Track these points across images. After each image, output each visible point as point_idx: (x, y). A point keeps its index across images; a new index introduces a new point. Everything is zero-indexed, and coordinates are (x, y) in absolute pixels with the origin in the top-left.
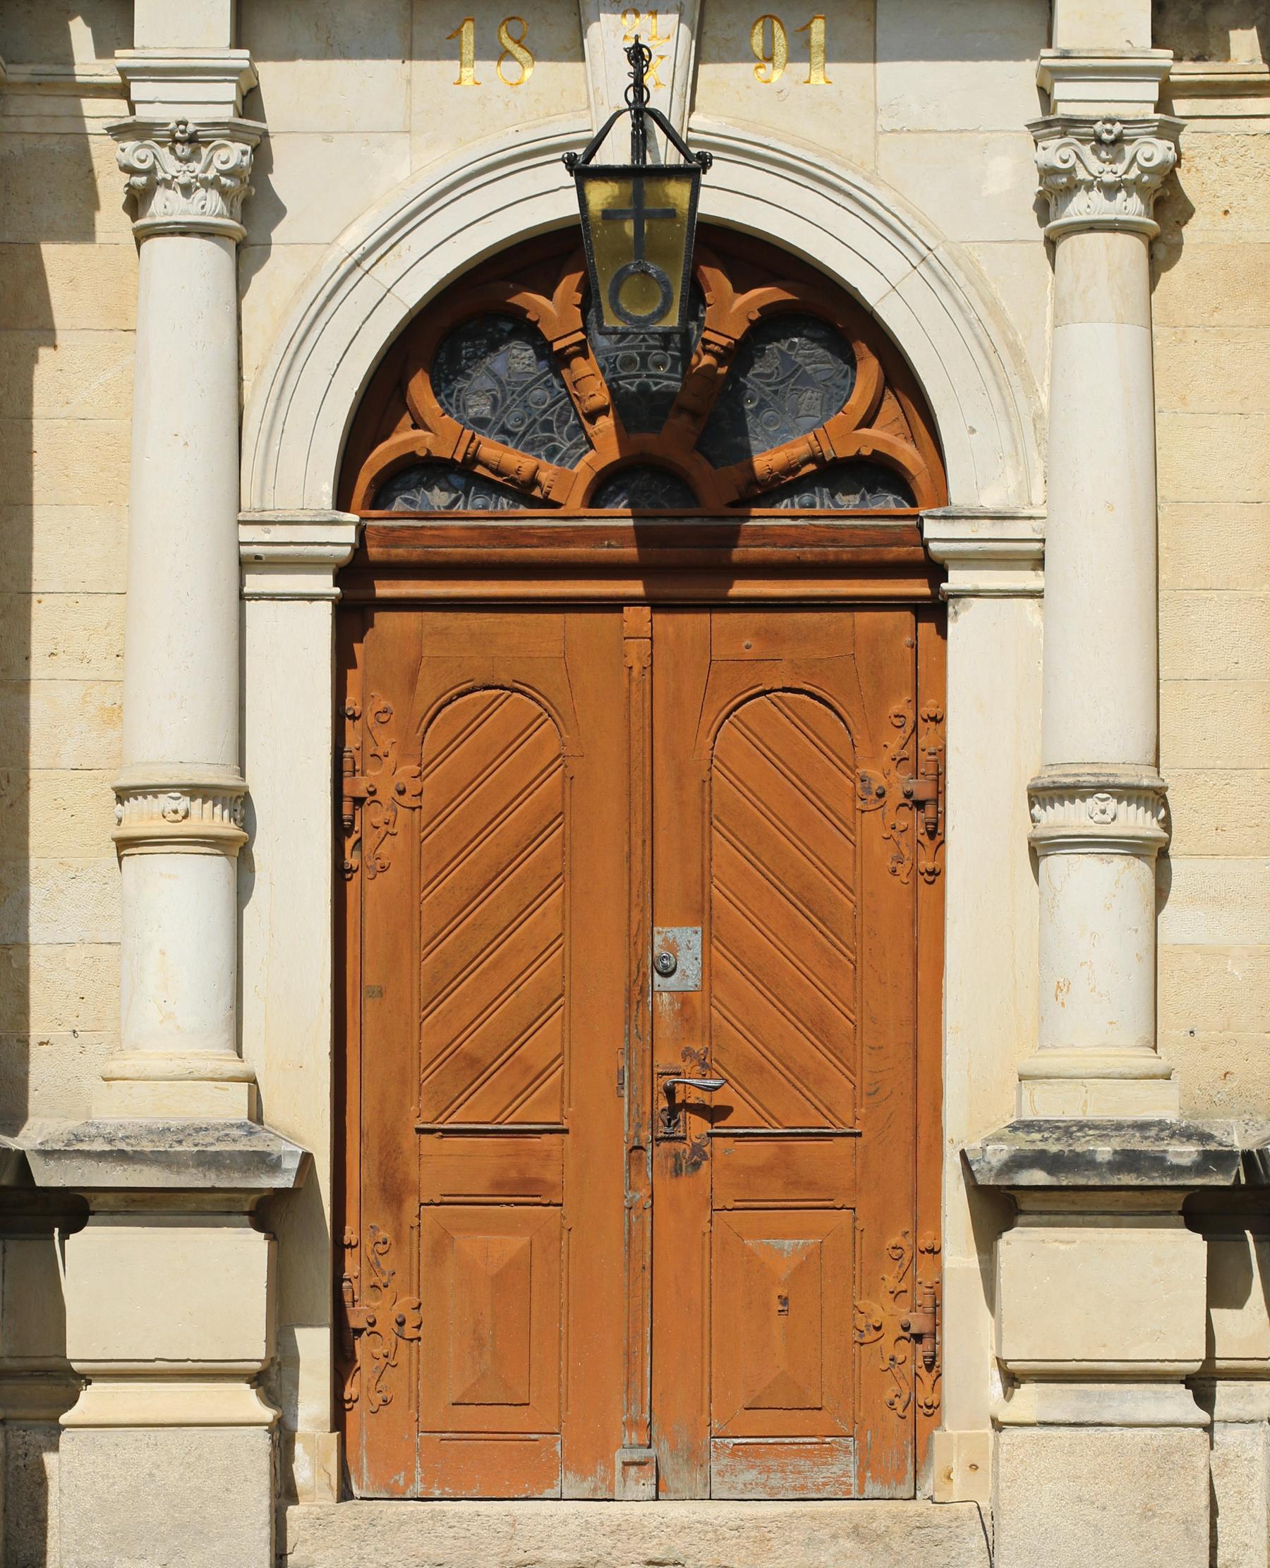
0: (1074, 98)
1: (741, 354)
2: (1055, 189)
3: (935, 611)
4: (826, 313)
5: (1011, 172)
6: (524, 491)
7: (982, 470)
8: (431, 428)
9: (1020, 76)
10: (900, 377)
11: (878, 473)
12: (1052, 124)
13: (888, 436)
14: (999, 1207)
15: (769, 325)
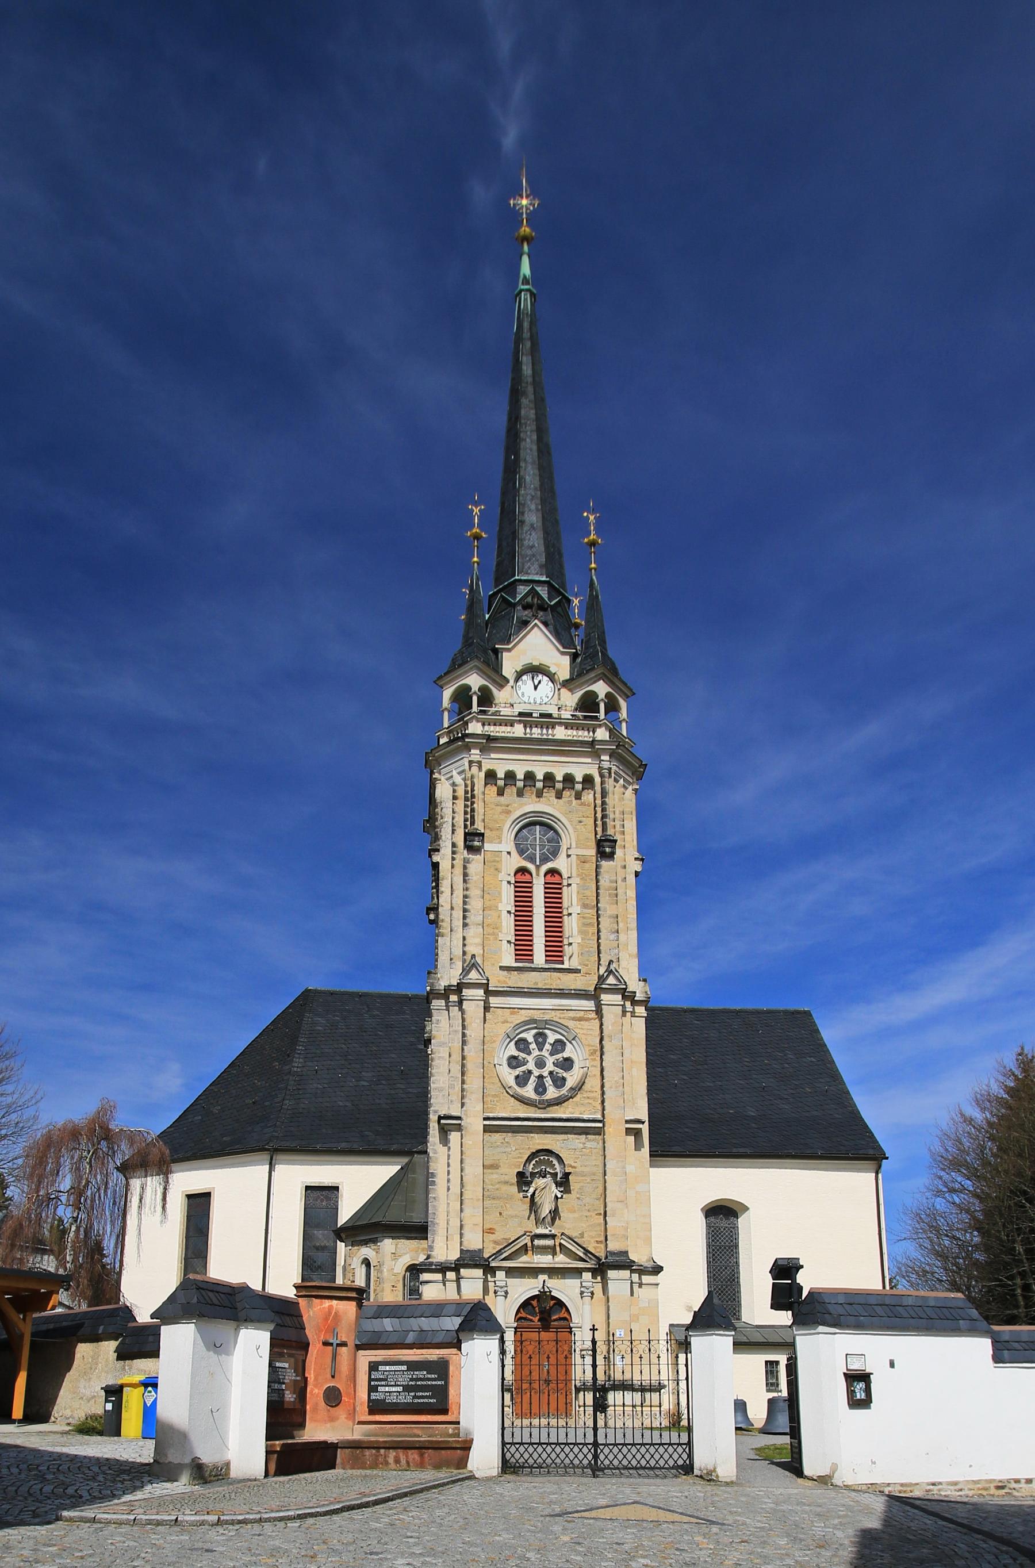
0: (584, 1284)
1: (551, 1308)
2: (582, 1293)
3: (571, 1332)
4: (560, 1304)
5: (578, 1291)
6: (531, 1320)
7: (576, 1320)
8: (523, 1315)
9: (579, 1281)
10: (567, 1310)
11: (565, 1319)
12: (582, 1286)
13: (566, 1315)
14: (578, 1390)
15: (555, 1304)
